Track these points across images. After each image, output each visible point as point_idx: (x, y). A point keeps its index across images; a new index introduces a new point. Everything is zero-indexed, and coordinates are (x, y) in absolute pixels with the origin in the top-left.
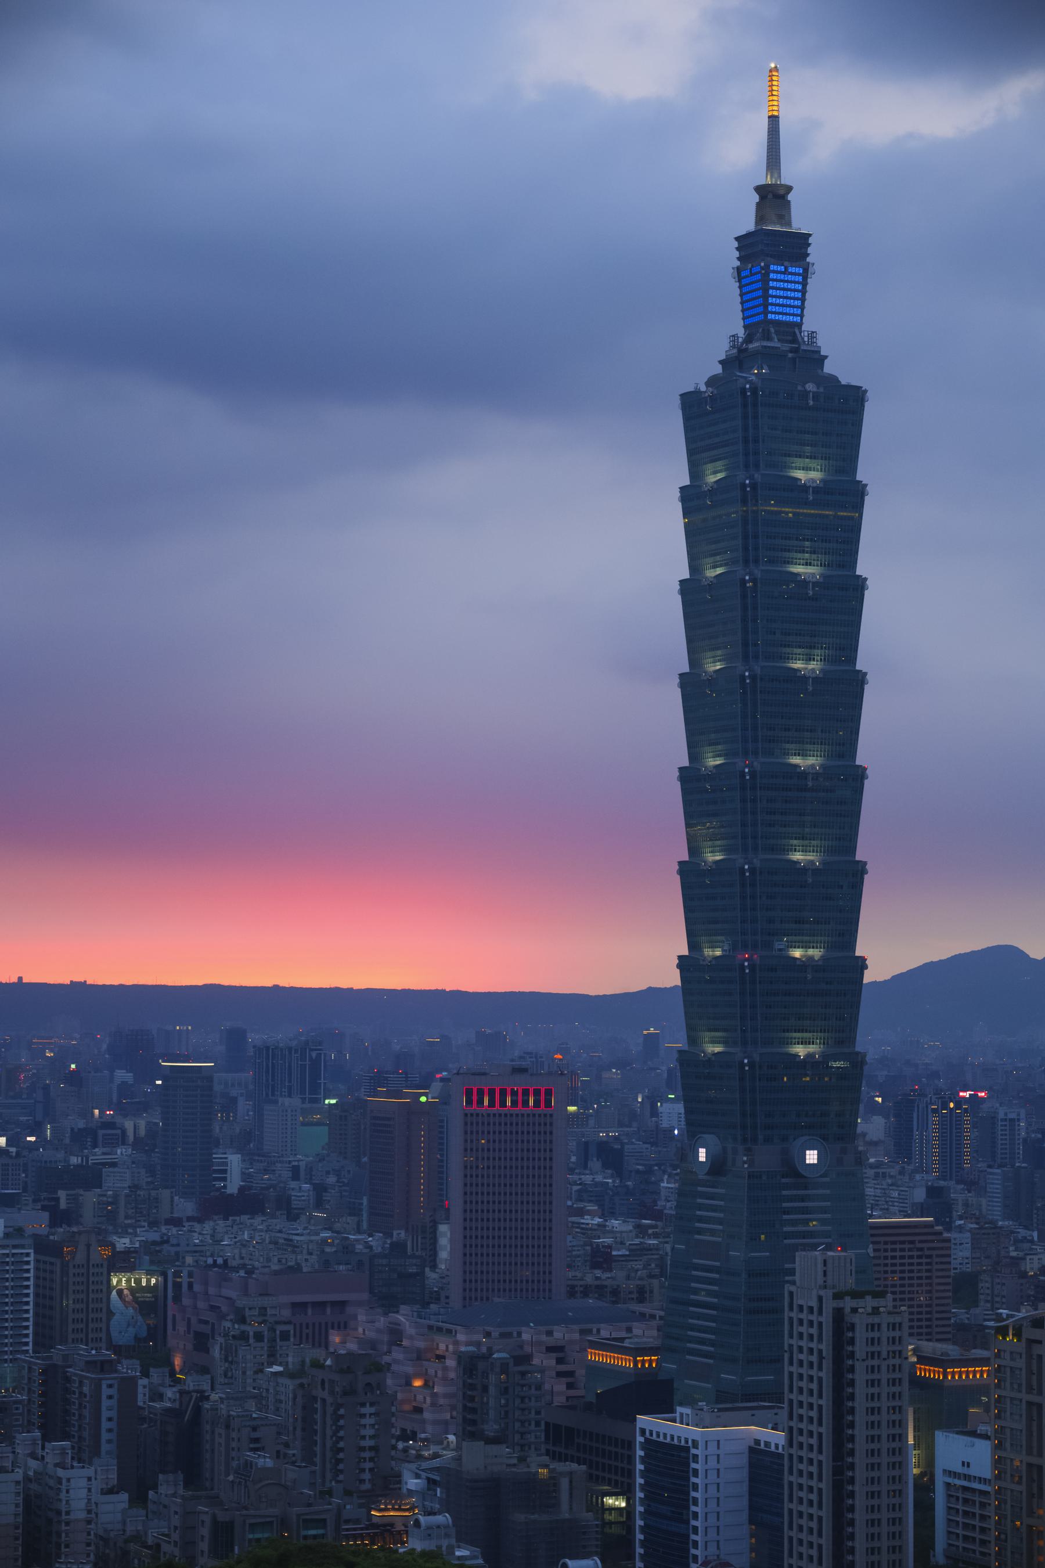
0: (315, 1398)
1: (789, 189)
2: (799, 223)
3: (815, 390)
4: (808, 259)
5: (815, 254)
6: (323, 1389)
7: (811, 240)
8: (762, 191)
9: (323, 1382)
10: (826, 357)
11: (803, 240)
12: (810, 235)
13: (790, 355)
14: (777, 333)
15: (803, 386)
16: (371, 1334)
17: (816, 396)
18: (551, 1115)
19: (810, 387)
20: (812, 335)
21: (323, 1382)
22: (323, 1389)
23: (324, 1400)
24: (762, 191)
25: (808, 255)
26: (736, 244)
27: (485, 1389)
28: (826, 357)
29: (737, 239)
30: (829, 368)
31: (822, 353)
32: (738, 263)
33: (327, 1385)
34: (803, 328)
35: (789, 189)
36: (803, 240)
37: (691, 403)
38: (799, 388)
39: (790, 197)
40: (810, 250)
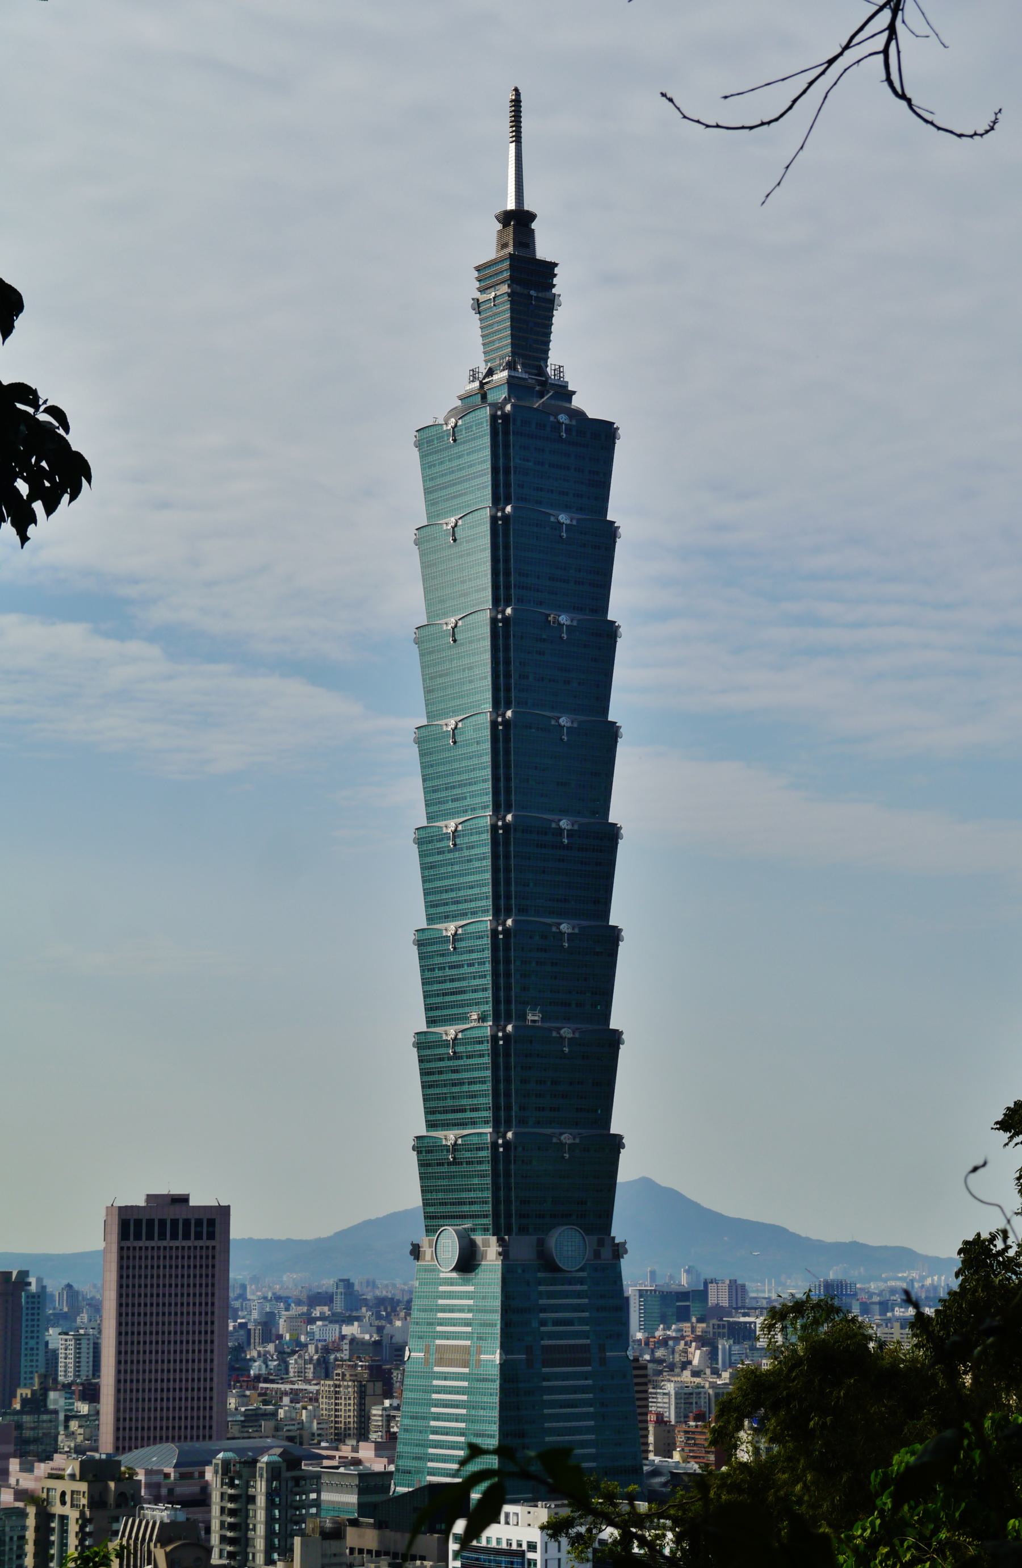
0: (52, 1516)
1: (532, 217)
2: (543, 251)
3: (567, 422)
4: (554, 291)
5: (561, 285)
6: (63, 1503)
7: (556, 270)
8: (506, 218)
9: (63, 1494)
10: (574, 393)
11: (548, 269)
12: (556, 265)
13: (538, 388)
14: (523, 366)
15: (556, 417)
16: (27, 1482)
17: (569, 429)
18: (214, 1248)
19: (563, 418)
20: (559, 369)
21: (63, 1494)
22: (63, 1503)
23: (63, 1518)
24: (506, 218)
25: (554, 286)
26: (476, 274)
27: (252, 1499)
28: (574, 393)
29: (478, 269)
30: (576, 402)
31: (570, 388)
32: (477, 295)
33: (68, 1498)
34: (549, 362)
35: (532, 217)
36: (548, 269)
37: (428, 440)
38: (552, 419)
39: (534, 226)
40: (555, 281)
